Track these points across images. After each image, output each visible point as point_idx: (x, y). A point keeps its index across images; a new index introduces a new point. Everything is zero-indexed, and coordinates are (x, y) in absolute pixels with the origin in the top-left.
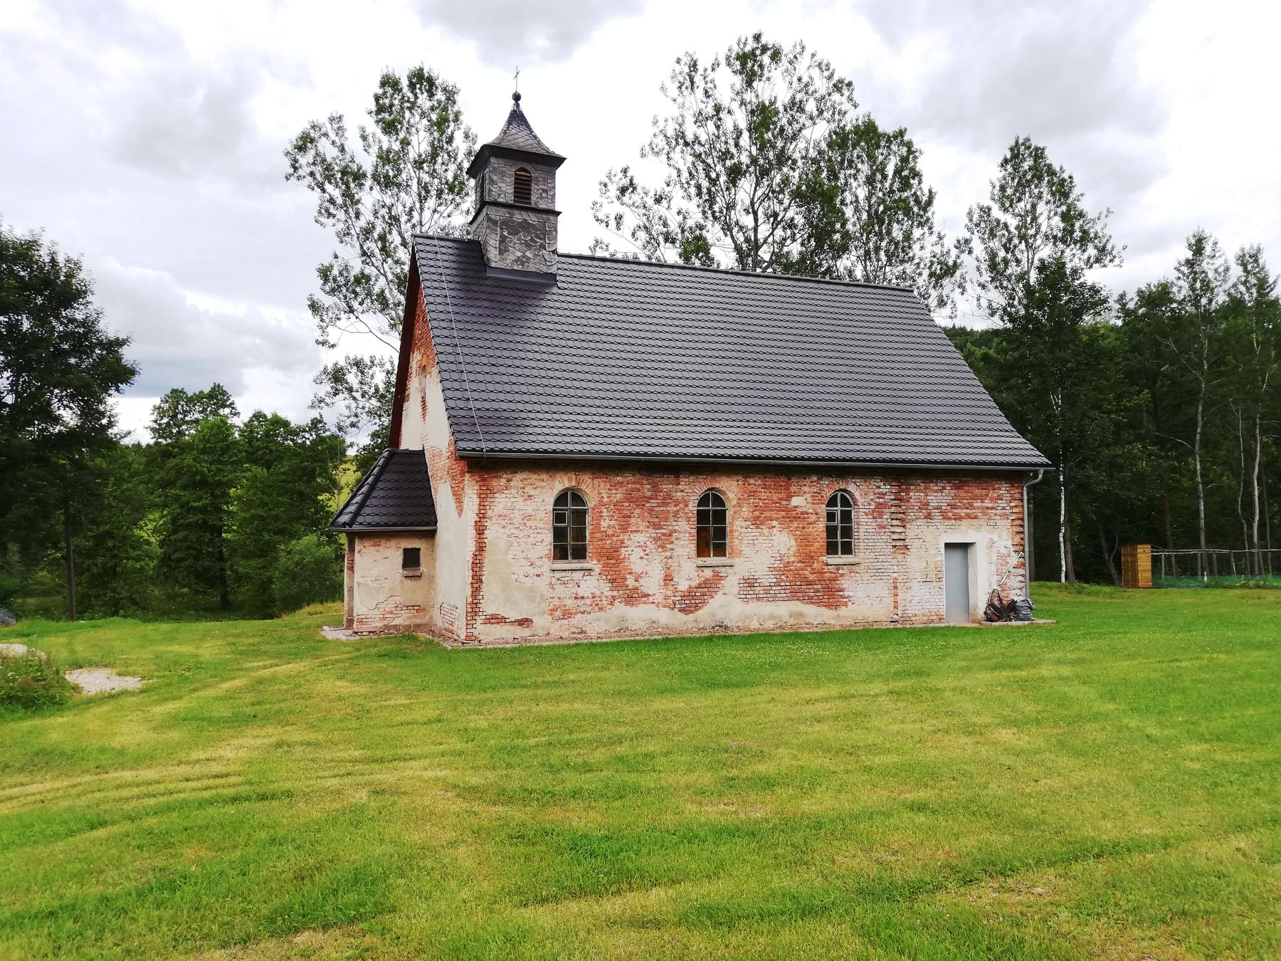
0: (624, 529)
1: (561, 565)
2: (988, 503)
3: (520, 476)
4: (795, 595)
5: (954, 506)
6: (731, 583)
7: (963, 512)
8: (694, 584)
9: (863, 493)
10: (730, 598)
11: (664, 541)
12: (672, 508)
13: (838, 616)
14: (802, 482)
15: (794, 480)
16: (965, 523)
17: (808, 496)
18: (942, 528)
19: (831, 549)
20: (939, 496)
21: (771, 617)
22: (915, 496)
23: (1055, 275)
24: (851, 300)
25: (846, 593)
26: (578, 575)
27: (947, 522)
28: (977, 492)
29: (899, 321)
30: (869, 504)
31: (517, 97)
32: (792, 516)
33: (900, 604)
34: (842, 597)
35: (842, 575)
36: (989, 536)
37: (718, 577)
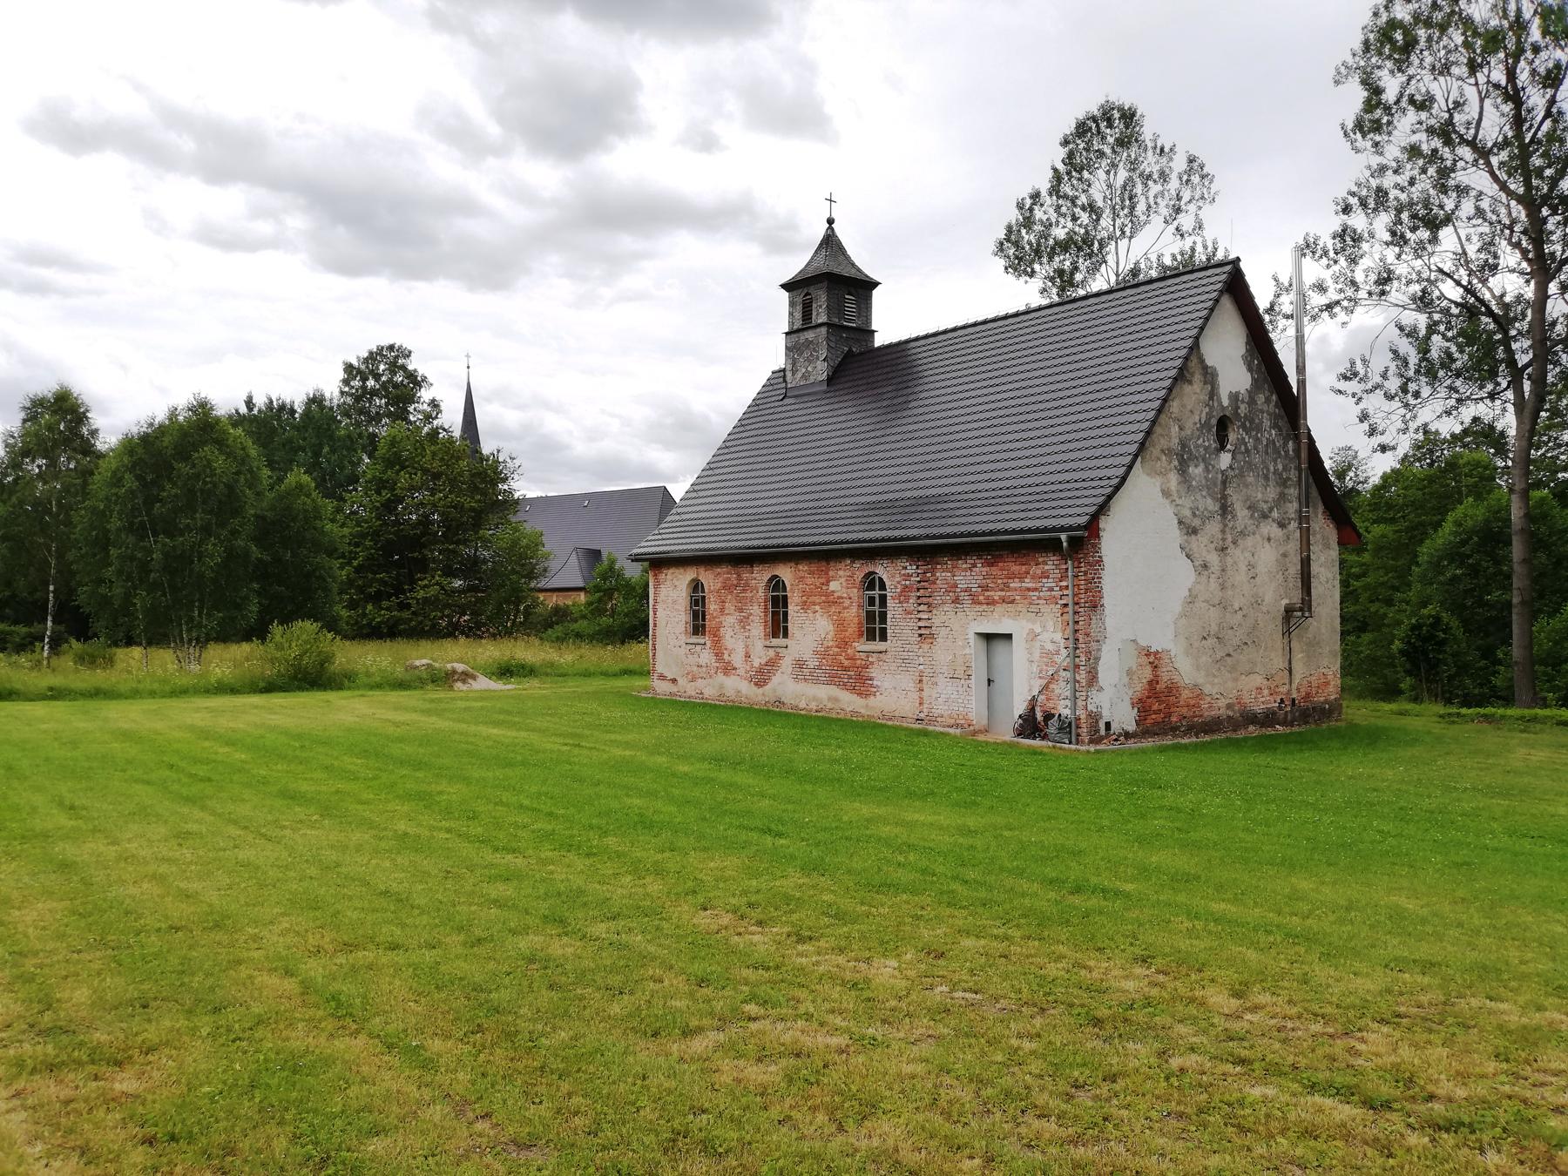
0: (722, 610)
1: (694, 639)
2: (1028, 583)
3: (671, 571)
4: (832, 680)
5: (985, 588)
6: (787, 664)
7: (996, 595)
9: (892, 574)
10: (785, 676)
11: (744, 622)
12: (749, 594)
14: (839, 566)
15: (832, 564)
16: (999, 608)
17: (843, 580)
18: (972, 615)
19: (871, 636)
20: (968, 575)
21: (815, 699)
22: (942, 576)
23: (1409, 159)
24: (1015, 333)
26: (698, 647)
27: (978, 608)
28: (1015, 568)
31: (830, 221)
32: (831, 601)
33: (926, 700)
34: (871, 686)
35: (872, 663)
36: (1030, 626)
37: (778, 657)
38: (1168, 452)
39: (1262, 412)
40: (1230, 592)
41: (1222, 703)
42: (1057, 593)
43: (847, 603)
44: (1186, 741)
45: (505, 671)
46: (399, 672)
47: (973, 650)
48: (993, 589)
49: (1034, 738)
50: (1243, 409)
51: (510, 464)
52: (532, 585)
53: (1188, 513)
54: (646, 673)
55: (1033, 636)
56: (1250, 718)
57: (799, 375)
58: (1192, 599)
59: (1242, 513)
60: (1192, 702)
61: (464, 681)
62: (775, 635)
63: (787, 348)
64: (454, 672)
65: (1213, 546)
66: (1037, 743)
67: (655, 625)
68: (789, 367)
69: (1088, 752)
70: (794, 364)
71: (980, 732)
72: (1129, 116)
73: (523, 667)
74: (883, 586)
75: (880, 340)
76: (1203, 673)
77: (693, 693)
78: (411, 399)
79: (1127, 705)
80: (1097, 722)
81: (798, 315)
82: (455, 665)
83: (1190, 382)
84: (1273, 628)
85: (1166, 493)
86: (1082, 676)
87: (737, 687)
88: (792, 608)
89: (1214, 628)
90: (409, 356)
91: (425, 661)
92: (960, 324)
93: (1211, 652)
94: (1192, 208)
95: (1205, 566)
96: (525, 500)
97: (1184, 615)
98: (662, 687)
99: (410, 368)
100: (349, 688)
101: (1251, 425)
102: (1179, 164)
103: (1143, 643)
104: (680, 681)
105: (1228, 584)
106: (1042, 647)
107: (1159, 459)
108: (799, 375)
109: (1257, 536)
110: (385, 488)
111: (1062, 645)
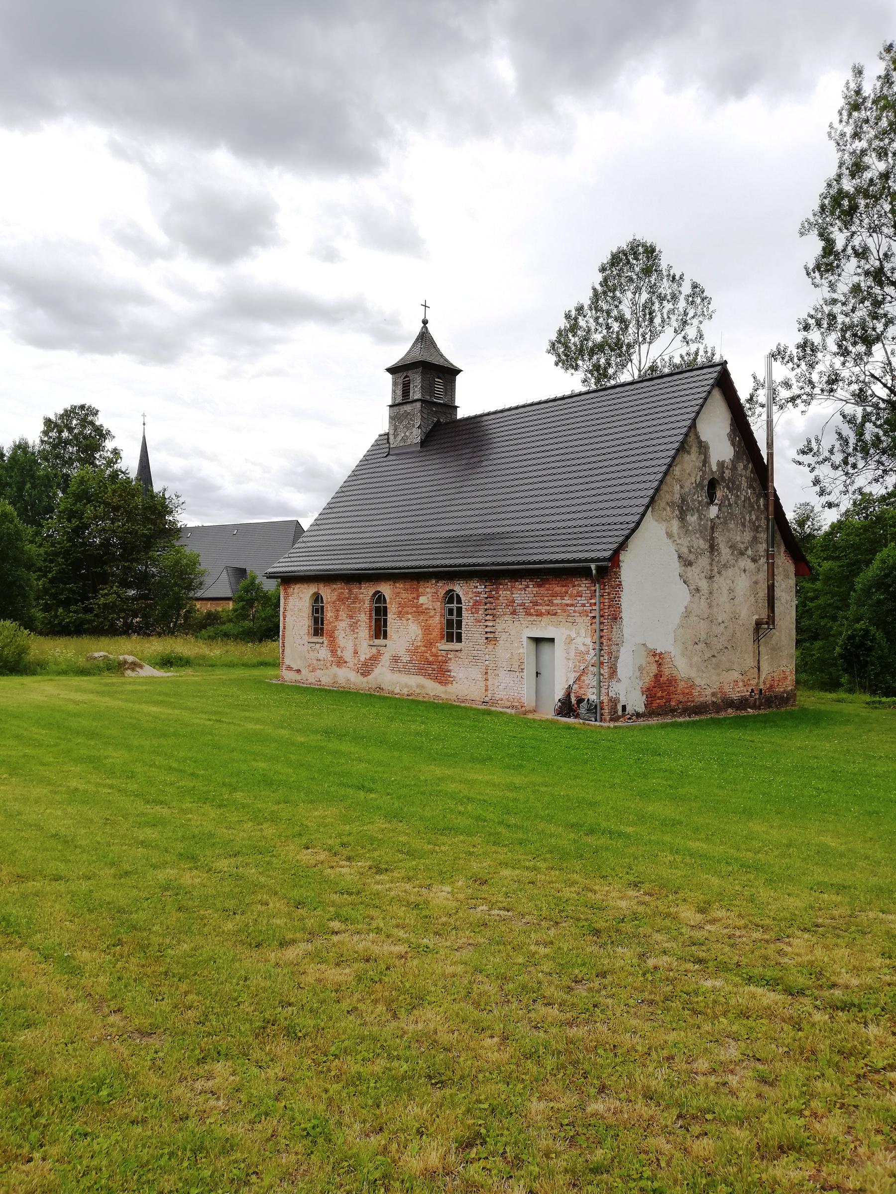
0: (337, 617)
1: (315, 639)
2: (567, 601)
3: (298, 586)
4: (421, 671)
5: (535, 604)
6: (385, 659)
7: (544, 609)
8: (368, 657)
11: (354, 627)
12: (357, 605)
13: (446, 692)
15: (421, 583)
16: (546, 619)
17: (429, 595)
18: (525, 623)
19: (450, 639)
21: (406, 686)
22: (504, 594)
25: (452, 674)
26: (318, 646)
28: (558, 589)
29: (550, 430)
30: (469, 602)
31: (425, 322)
32: (420, 611)
35: (450, 659)
36: (568, 632)
37: (379, 653)
38: (671, 504)
39: (741, 476)
41: (709, 692)
42: (588, 608)
43: (432, 613)
44: (681, 720)
45: (167, 662)
46: (81, 661)
47: (526, 649)
48: (541, 605)
49: (570, 717)
50: (727, 474)
51: (175, 501)
52: (191, 594)
53: (685, 550)
54: (276, 665)
55: (570, 640)
56: (729, 704)
57: (399, 438)
58: (687, 614)
59: (725, 551)
60: (687, 691)
61: (133, 670)
62: (377, 637)
63: (391, 417)
64: (125, 662)
65: (703, 575)
66: (571, 720)
67: (284, 628)
68: (392, 432)
69: (609, 727)
70: (395, 430)
71: (530, 711)
72: (650, 251)
73: (181, 659)
74: (459, 601)
75: (461, 414)
77: (313, 681)
78: (97, 448)
79: (638, 692)
80: (616, 705)
81: (399, 392)
82: (126, 657)
83: (689, 453)
84: (749, 636)
85: (670, 535)
86: (605, 671)
87: (348, 676)
88: (390, 617)
89: (703, 636)
90: (96, 414)
91: (102, 654)
92: (521, 404)
94: (695, 322)
95: (698, 590)
96: (187, 529)
97: (681, 626)
98: (289, 676)
99: (97, 423)
100: (41, 674)
101: (733, 486)
102: (686, 289)
103: (651, 646)
104: (303, 671)
105: (714, 604)
106: (577, 648)
107: (665, 509)
108: (399, 438)
109: (736, 568)
110: (75, 517)
111: (591, 647)
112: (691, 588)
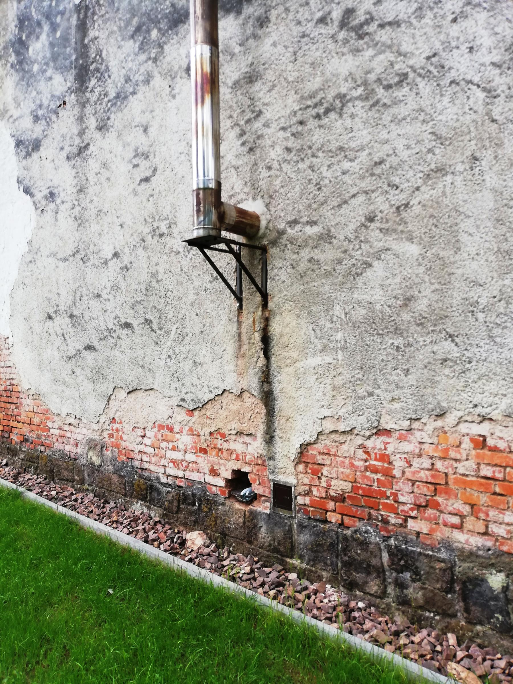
40: (94, 228)
60: (37, 420)
76: (48, 376)
93: (58, 341)
105: (92, 211)
109: (157, 81)
112: (39, 196)
